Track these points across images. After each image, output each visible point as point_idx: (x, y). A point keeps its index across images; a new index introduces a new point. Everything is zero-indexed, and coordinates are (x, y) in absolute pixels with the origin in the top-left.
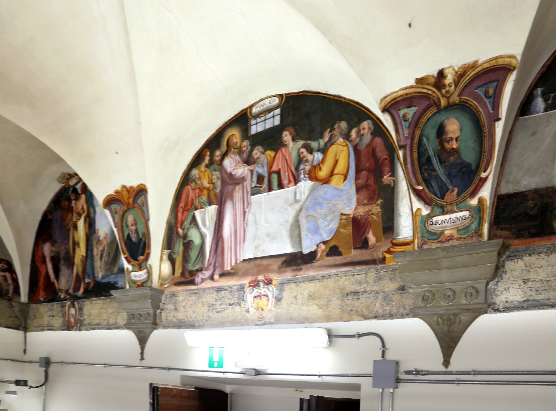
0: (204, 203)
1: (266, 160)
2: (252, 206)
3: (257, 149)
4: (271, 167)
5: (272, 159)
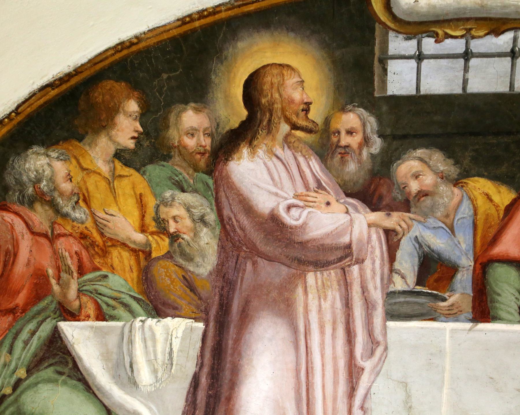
0: (115, 299)
1: (466, 210)
2: (392, 354)
3: (421, 160)
4: (495, 240)
5: (496, 216)
